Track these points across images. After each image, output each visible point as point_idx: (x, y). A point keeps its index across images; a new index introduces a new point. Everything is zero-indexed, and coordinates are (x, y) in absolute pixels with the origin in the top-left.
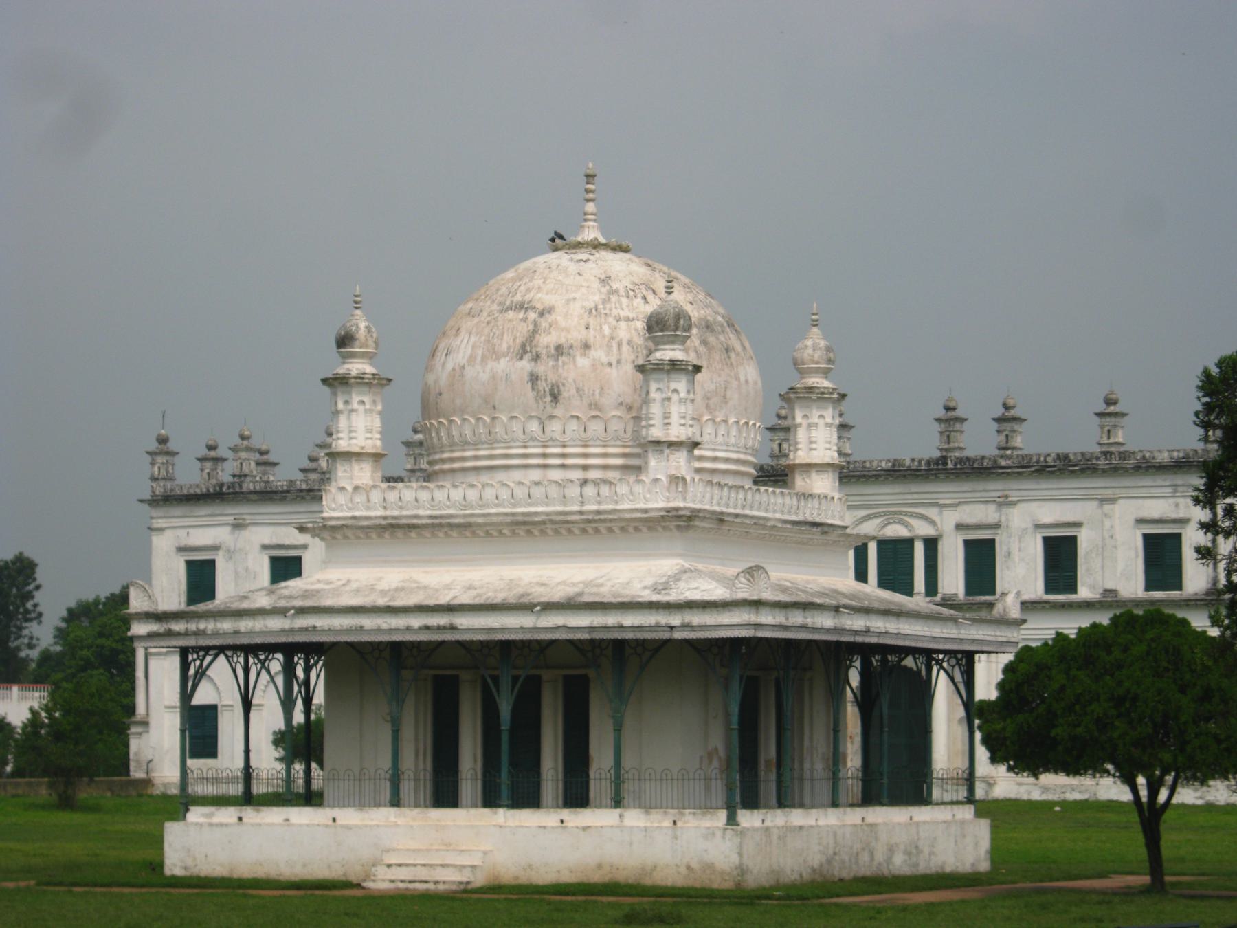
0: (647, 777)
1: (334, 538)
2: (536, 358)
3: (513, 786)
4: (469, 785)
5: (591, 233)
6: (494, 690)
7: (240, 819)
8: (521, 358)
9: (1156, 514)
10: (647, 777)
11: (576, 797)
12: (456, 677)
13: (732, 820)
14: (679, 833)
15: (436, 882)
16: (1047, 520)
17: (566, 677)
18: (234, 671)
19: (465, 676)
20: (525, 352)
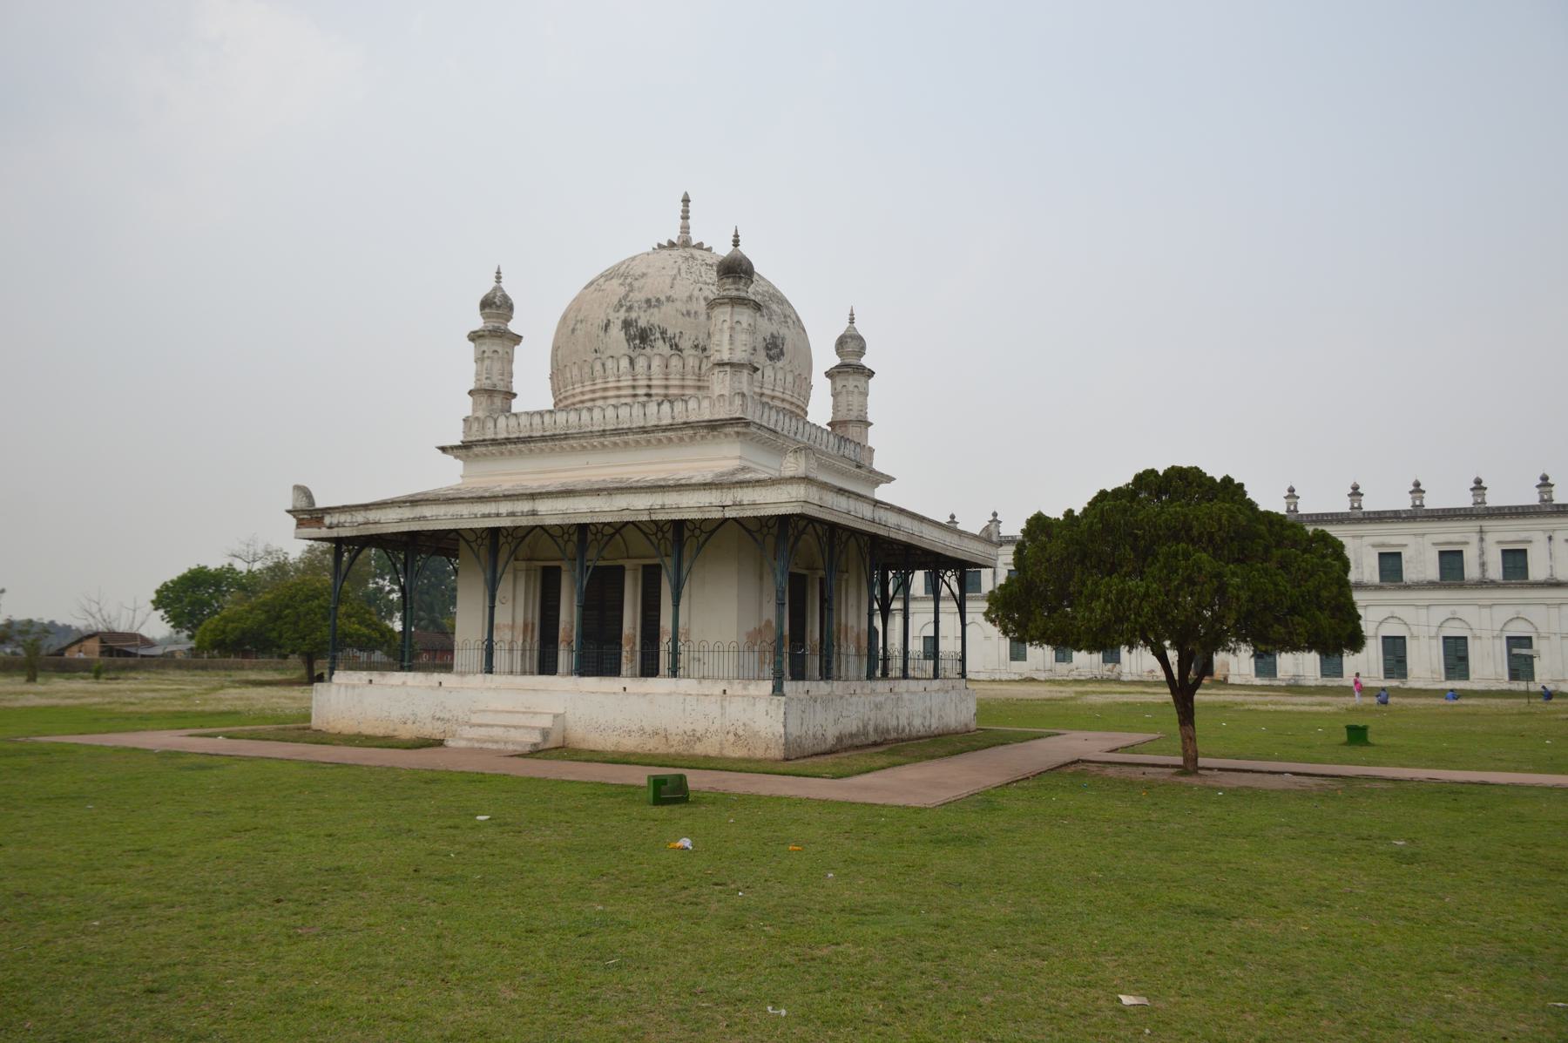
2: (630, 309)
3: (599, 659)
12: (559, 568)
13: (778, 690)
14: (726, 704)
17: (645, 567)
19: (565, 566)
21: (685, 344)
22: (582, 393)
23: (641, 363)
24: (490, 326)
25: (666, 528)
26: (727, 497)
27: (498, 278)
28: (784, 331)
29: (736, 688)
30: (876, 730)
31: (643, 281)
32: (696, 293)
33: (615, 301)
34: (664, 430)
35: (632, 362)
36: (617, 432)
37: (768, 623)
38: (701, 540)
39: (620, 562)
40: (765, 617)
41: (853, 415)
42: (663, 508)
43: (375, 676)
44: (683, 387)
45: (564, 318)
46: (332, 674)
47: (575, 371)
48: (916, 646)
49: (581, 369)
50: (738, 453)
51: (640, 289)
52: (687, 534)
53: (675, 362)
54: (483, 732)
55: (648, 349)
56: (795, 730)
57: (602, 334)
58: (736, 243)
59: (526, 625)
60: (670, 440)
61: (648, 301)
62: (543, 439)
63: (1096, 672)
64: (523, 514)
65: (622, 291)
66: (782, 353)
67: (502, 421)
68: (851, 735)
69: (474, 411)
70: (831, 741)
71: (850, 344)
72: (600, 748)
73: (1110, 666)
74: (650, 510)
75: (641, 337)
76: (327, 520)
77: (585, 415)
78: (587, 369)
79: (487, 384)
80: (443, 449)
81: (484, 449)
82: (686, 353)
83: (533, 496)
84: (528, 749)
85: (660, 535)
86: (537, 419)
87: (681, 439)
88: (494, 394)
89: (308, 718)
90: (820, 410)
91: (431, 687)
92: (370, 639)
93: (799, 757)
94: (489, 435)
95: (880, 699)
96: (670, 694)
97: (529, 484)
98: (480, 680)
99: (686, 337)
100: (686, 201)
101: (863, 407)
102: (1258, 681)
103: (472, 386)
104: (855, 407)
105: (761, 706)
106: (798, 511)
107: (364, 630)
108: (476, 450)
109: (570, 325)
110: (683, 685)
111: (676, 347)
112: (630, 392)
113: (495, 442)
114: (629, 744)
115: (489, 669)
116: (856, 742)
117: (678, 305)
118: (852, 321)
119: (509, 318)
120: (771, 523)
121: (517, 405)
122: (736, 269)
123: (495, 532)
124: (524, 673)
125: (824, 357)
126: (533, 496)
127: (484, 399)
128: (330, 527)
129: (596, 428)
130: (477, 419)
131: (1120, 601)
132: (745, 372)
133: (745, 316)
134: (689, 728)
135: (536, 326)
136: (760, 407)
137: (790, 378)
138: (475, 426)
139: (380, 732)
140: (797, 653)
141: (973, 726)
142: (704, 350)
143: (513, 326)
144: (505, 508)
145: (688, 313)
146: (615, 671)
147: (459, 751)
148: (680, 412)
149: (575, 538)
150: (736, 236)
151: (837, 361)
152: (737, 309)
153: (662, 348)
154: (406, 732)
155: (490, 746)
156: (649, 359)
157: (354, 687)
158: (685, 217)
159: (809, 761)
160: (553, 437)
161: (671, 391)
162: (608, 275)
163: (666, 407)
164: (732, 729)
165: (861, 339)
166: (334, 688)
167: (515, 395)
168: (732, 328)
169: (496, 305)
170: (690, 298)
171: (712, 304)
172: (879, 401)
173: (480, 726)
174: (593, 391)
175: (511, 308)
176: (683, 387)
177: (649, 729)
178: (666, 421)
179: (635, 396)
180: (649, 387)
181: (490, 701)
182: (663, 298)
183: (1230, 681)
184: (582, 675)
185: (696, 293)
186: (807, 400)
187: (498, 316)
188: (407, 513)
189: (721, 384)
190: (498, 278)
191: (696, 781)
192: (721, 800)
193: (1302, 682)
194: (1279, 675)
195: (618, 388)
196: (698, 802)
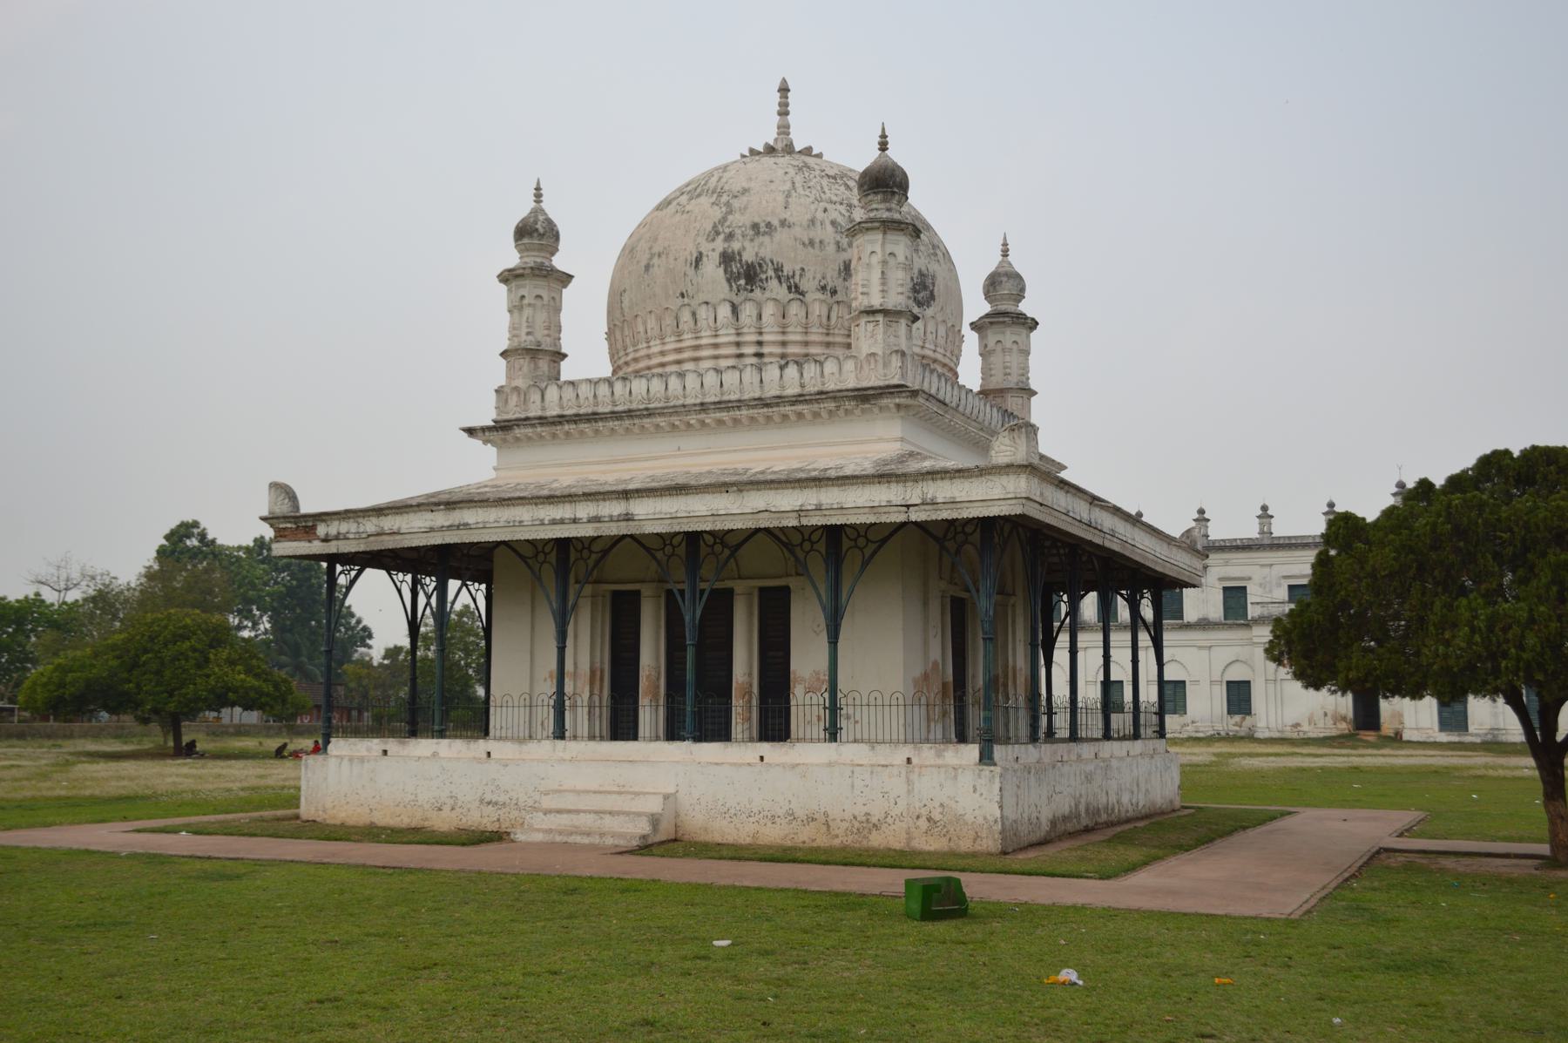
1: (505, 441)
3: (699, 715)
4: (649, 715)
7: (385, 752)
11: (775, 727)
12: (637, 593)
13: (986, 758)
14: (914, 777)
15: (602, 835)
17: (762, 590)
18: (399, 591)
19: (646, 591)
20: (718, 233)
21: (808, 284)
22: (662, 353)
23: (748, 311)
24: (531, 261)
25: (815, 537)
26: (914, 494)
27: (538, 196)
28: (934, 267)
29: (927, 754)
30: (1087, 810)
31: (744, 199)
32: (820, 215)
33: (709, 228)
34: (793, 403)
35: (735, 310)
36: (721, 405)
37: (935, 663)
38: (868, 552)
39: (728, 584)
40: (932, 659)
41: (1012, 381)
42: (819, 508)
43: (392, 745)
44: (806, 344)
45: (629, 251)
46: (327, 742)
47: (652, 323)
48: (1090, 692)
49: (660, 319)
50: (899, 434)
51: (743, 210)
52: (846, 543)
53: (795, 309)
54: (564, 820)
55: (758, 292)
56: (1011, 814)
57: (691, 272)
58: (883, 146)
59: (593, 672)
60: (800, 415)
61: (755, 226)
62: (616, 416)
63: (1219, 727)
65: (717, 214)
66: (932, 297)
67: (552, 393)
68: (1065, 819)
69: (509, 377)
70: (1045, 826)
71: (1004, 284)
72: (730, 839)
73: (1237, 718)
74: (800, 512)
75: (748, 276)
76: (321, 530)
77: (674, 383)
78: (669, 321)
79: (527, 341)
80: (471, 431)
81: (529, 431)
82: (809, 297)
83: (626, 495)
84: (635, 843)
85: (807, 545)
86: (603, 390)
87: (816, 415)
88: (537, 354)
89: (294, 801)
90: (970, 373)
91: (478, 760)
92: (261, 694)
93: (1021, 848)
94: (534, 411)
95: (1090, 767)
96: (830, 765)
97: (603, 478)
98: (545, 748)
99: (809, 275)
100: (784, 90)
101: (1025, 371)
102: (1444, 737)
103: (505, 345)
104: (1015, 371)
105: (966, 779)
106: (1018, 510)
107: (252, 681)
108: (517, 432)
109: (639, 260)
110: (847, 752)
111: (795, 289)
112: (733, 350)
113: (543, 420)
114: (773, 834)
115: (560, 734)
116: (1070, 827)
118: (1005, 253)
119: (553, 250)
120: (969, 529)
121: (568, 371)
122: (885, 182)
123: (563, 544)
124: (592, 737)
125: (975, 306)
126: (626, 495)
127: (525, 363)
128: (326, 540)
129: (689, 401)
130: (516, 389)
131: (1490, 629)
132: (903, 322)
133: (900, 245)
134: (860, 811)
135: (589, 264)
136: (920, 370)
137: (942, 331)
138: (513, 400)
139: (404, 821)
140: (976, 703)
141: (1178, 804)
142: (834, 292)
143: (560, 262)
144: (584, 510)
145: (812, 243)
147: (529, 845)
148: (812, 377)
149: (553, 557)
150: (884, 136)
151: (986, 308)
152: (891, 236)
153: (777, 290)
154: (443, 822)
155: (578, 839)
156: (759, 306)
157: (362, 760)
158: (784, 112)
159: (1032, 854)
160: (630, 414)
161: (791, 350)
162: (694, 190)
163: (792, 371)
164: (924, 812)
165: (1018, 277)
166: (332, 762)
167: (565, 356)
168: (884, 263)
169: (536, 233)
170: (813, 221)
171: (855, 230)
172: (1046, 359)
173: (559, 812)
174: (679, 350)
175: (557, 237)
176: (806, 344)
177: (801, 814)
178: (793, 390)
179: (740, 356)
180: (760, 343)
181: (559, 780)
182: (775, 222)
183: (1406, 737)
186: (957, 365)
187: (541, 248)
188: (440, 519)
189: (870, 338)
190: (538, 196)
191: (976, 887)
192: (999, 912)
193: (1503, 738)
194: (1471, 729)
195: (716, 346)
196: (974, 917)
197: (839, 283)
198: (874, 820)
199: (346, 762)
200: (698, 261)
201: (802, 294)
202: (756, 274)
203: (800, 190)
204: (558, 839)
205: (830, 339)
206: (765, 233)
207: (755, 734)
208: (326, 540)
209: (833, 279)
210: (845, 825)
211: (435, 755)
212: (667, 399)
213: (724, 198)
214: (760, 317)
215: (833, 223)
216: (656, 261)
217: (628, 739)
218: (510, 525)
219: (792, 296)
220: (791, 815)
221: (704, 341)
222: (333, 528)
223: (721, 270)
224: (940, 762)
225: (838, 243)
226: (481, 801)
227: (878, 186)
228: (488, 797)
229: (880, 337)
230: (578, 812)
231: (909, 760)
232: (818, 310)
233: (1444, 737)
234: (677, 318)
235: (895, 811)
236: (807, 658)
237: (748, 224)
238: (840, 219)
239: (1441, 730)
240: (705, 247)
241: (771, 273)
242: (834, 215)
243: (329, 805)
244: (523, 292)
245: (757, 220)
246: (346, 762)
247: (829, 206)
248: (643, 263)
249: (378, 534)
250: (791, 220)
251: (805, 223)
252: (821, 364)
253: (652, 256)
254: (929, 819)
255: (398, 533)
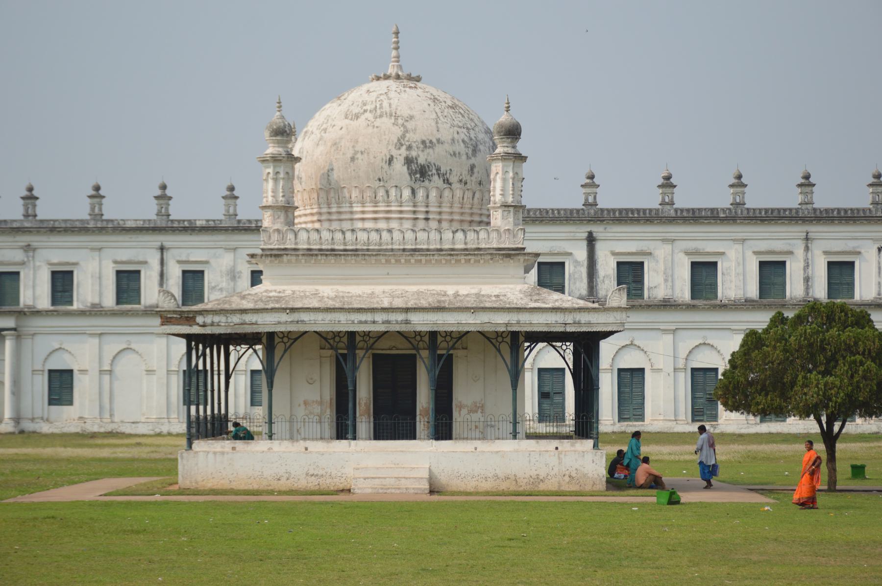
0: (501, 419)
5: (392, 70)
6: (343, 363)
8: (399, 149)
9: (124, 259)
10: (501, 419)
11: (443, 430)
14: (562, 456)
16: (55, 261)
20: (402, 145)
21: (454, 179)
23: (421, 194)
25: (504, 335)
26: (569, 318)
32: (456, 136)
33: (396, 141)
35: (413, 192)
42: (518, 323)
47: (355, 194)
49: (362, 192)
51: (414, 130)
53: (447, 193)
57: (386, 166)
61: (423, 142)
64: (397, 322)
65: (399, 131)
74: (507, 325)
75: (421, 172)
76: (200, 319)
78: (368, 194)
99: (454, 173)
105: (589, 457)
111: (447, 181)
117: (447, 146)
122: (513, 132)
126: (407, 310)
128: (204, 326)
134: (534, 473)
142: (466, 183)
144: (380, 317)
145: (455, 154)
146: (411, 435)
153: (437, 181)
157: (223, 453)
168: (513, 179)
170: (453, 140)
177: (501, 475)
182: (434, 141)
184: (437, 439)
185: (456, 136)
188: (284, 317)
197: (468, 178)
198: (541, 478)
199: (211, 456)
200: (390, 161)
201: (450, 184)
202: (426, 172)
203: (441, 118)
204: (381, 491)
205: (463, 211)
206: (430, 147)
207: (335, 435)
208: (204, 326)
209: (466, 176)
210: (526, 480)
211: (270, 449)
212: (380, 244)
213: (400, 121)
214: (428, 197)
215: (463, 141)
216: (359, 156)
217: (395, 439)
218: (331, 322)
219: (445, 186)
220: (496, 477)
221: (393, 208)
222: (209, 319)
223: (405, 168)
224: (573, 449)
225: (467, 154)
226: (307, 474)
227: (509, 134)
228: (311, 472)
229: (511, 220)
230: (385, 478)
231: (557, 448)
232: (458, 193)
233: (542, 428)
234: (375, 193)
235: (553, 473)
236: (464, 394)
237: (419, 140)
238: (466, 139)
239: (540, 420)
240: (395, 153)
241: (434, 171)
242: (462, 136)
243: (199, 479)
244: (277, 170)
245: (424, 138)
246: (211, 456)
247: (459, 130)
248: (349, 155)
249: (242, 324)
250: (442, 139)
251: (450, 141)
252: (478, 233)
253: (356, 153)
254: (570, 476)
255: (256, 324)
